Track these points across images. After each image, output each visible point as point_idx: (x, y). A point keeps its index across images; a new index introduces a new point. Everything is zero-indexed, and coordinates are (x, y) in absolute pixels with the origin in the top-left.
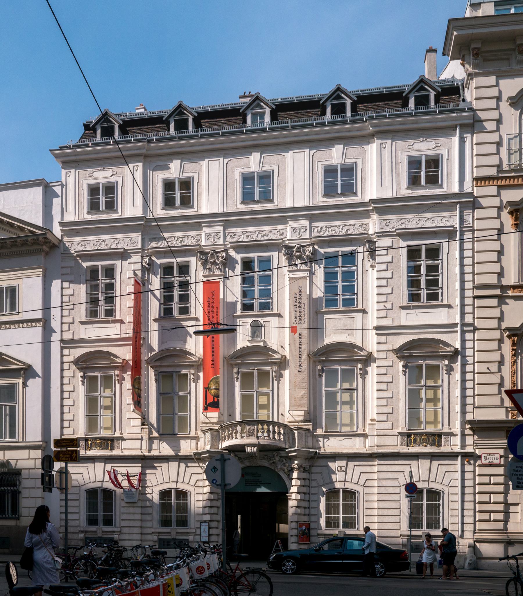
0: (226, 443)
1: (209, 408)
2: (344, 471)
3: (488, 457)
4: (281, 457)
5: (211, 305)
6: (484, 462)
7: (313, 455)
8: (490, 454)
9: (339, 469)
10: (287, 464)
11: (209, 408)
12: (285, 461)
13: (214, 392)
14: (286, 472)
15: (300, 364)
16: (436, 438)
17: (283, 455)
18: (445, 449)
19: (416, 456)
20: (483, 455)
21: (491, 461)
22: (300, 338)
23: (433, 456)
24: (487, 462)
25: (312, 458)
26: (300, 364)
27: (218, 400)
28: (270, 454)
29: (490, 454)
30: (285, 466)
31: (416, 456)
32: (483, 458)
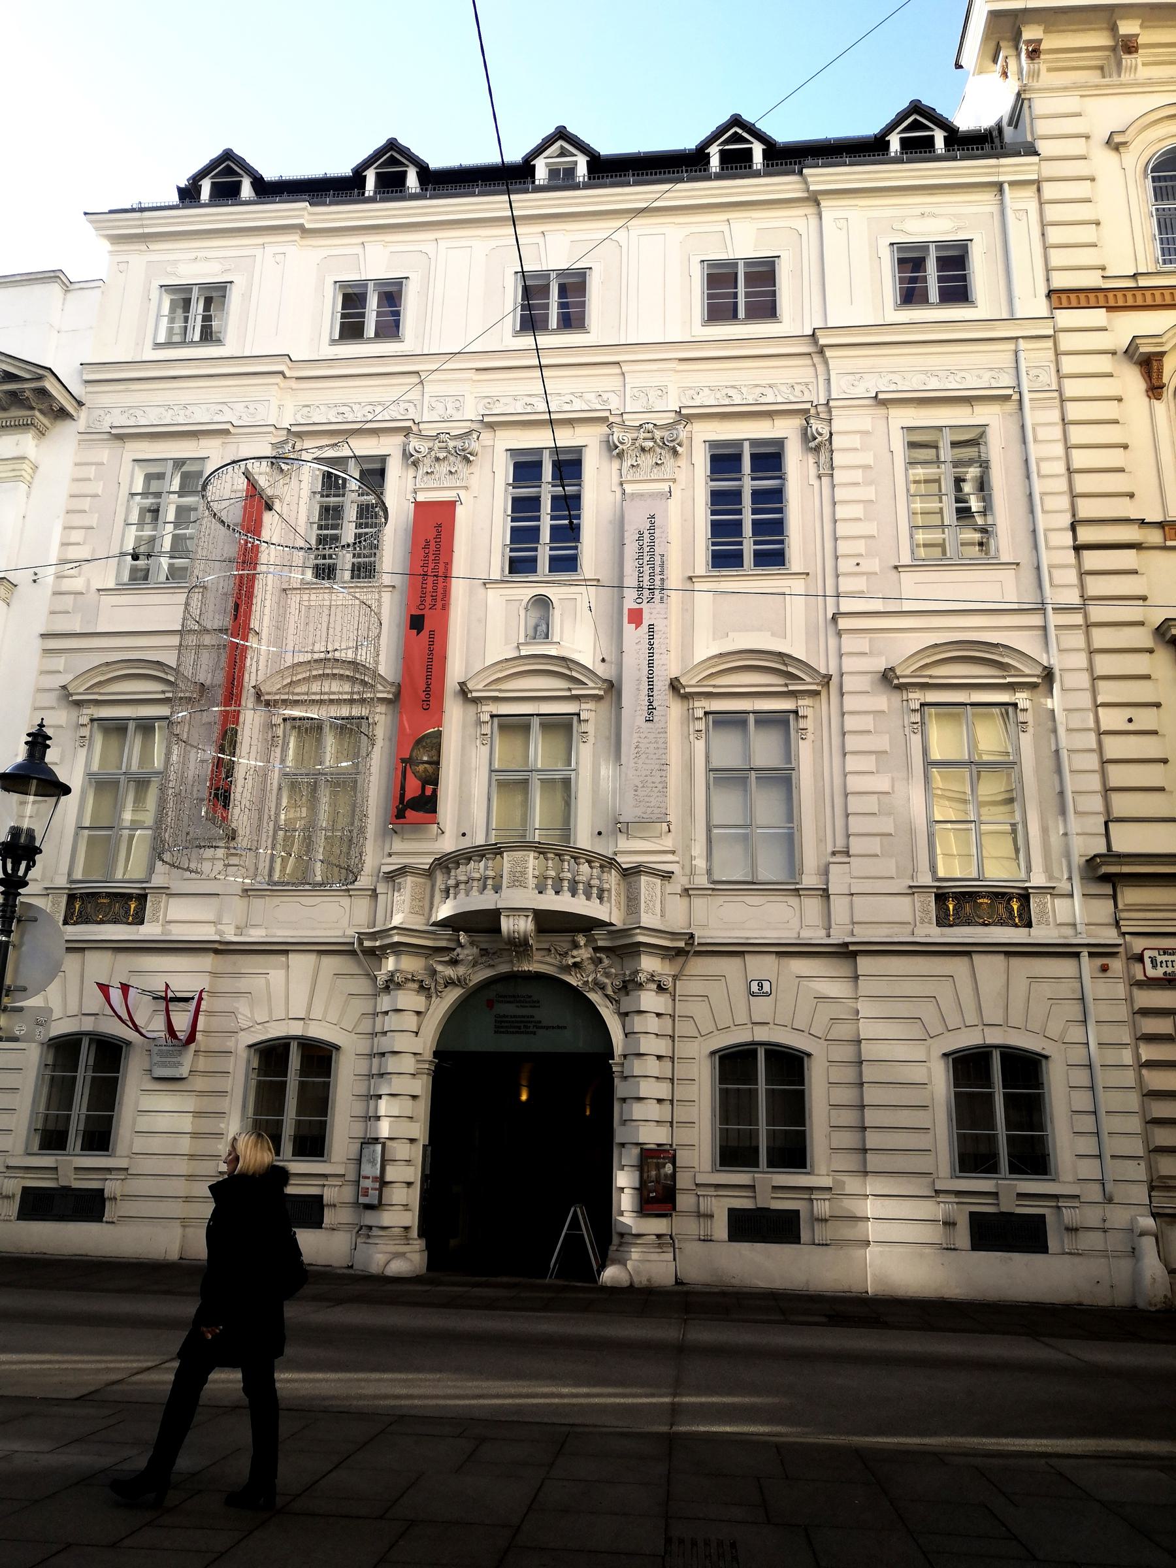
0: (445, 910)
1: (410, 814)
2: (768, 995)
3: (1159, 959)
4: (597, 949)
5: (432, 557)
6: (1151, 973)
7: (682, 944)
8: (1165, 952)
9: (755, 987)
10: (613, 970)
11: (410, 814)
12: (606, 962)
13: (426, 770)
14: (610, 992)
15: (651, 703)
16: (1013, 904)
17: (600, 943)
18: (1040, 934)
19: (964, 951)
20: (1147, 954)
21: (1169, 970)
22: (651, 637)
23: (1012, 952)
24: (1159, 973)
25: (679, 952)
26: (651, 703)
27: (435, 792)
28: (562, 942)
29: (1165, 952)
30: (607, 975)
31: (964, 951)
32: (1147, 961)
